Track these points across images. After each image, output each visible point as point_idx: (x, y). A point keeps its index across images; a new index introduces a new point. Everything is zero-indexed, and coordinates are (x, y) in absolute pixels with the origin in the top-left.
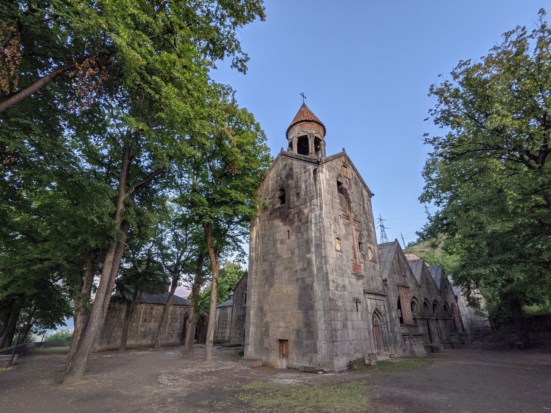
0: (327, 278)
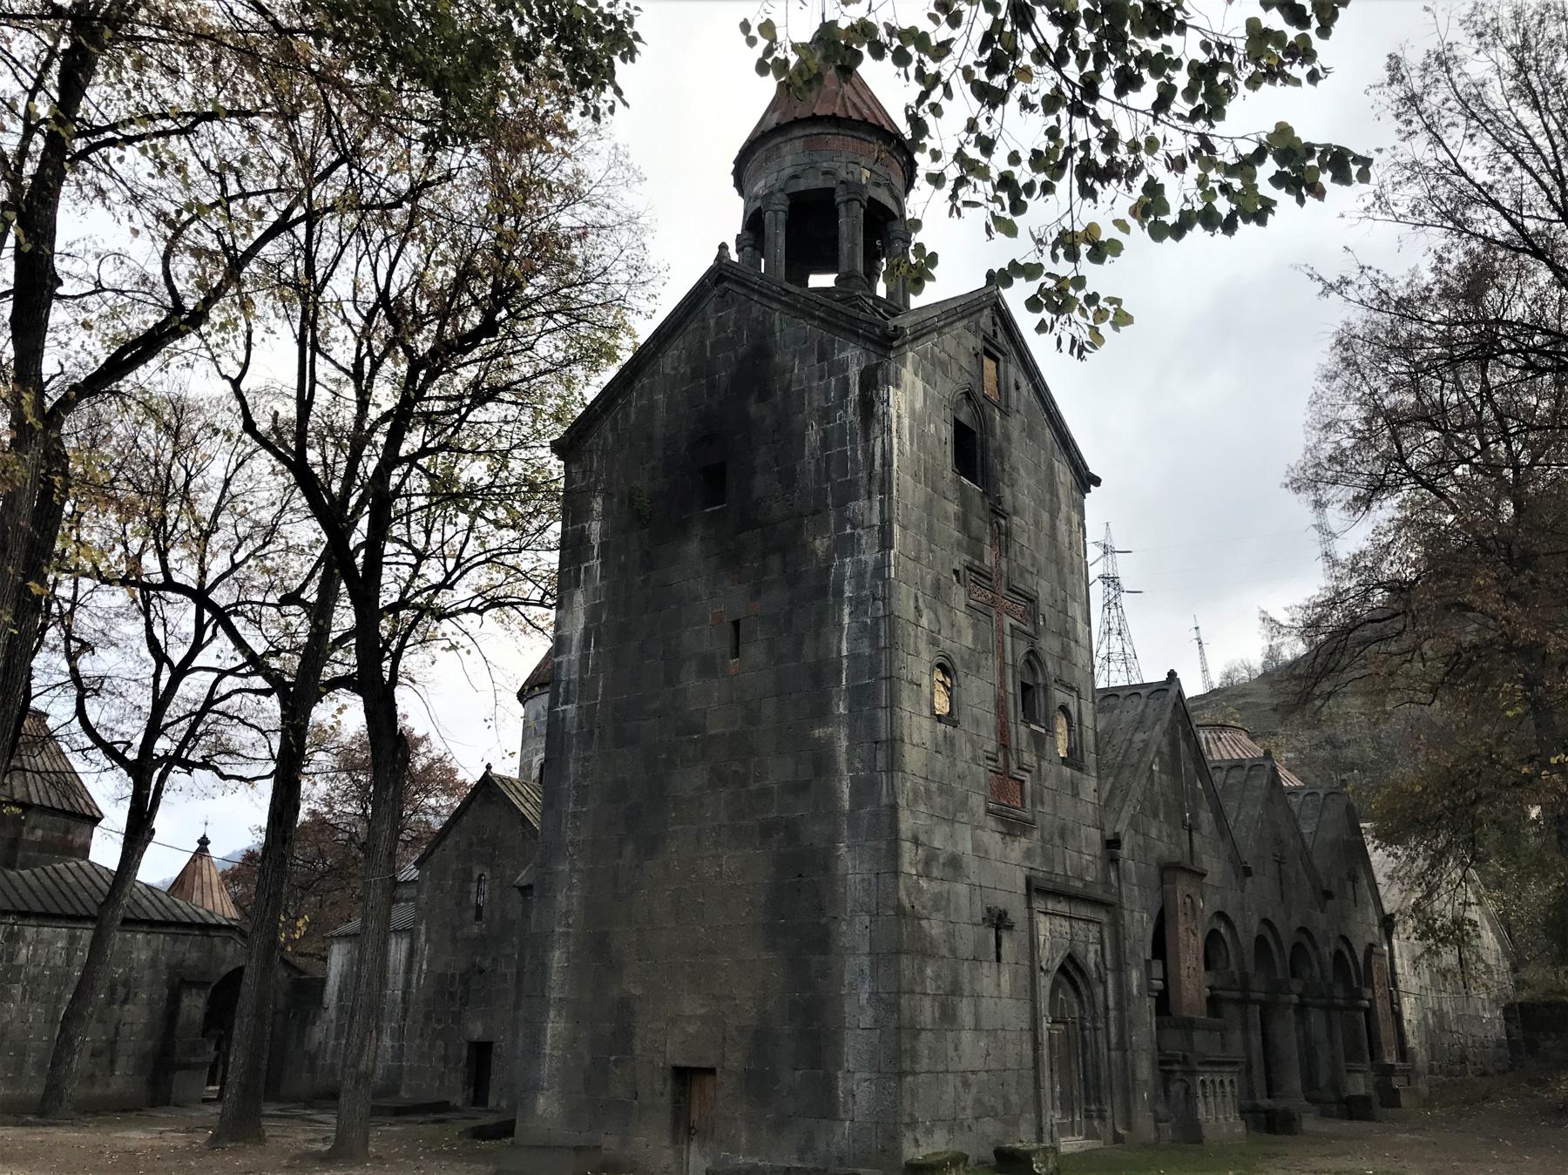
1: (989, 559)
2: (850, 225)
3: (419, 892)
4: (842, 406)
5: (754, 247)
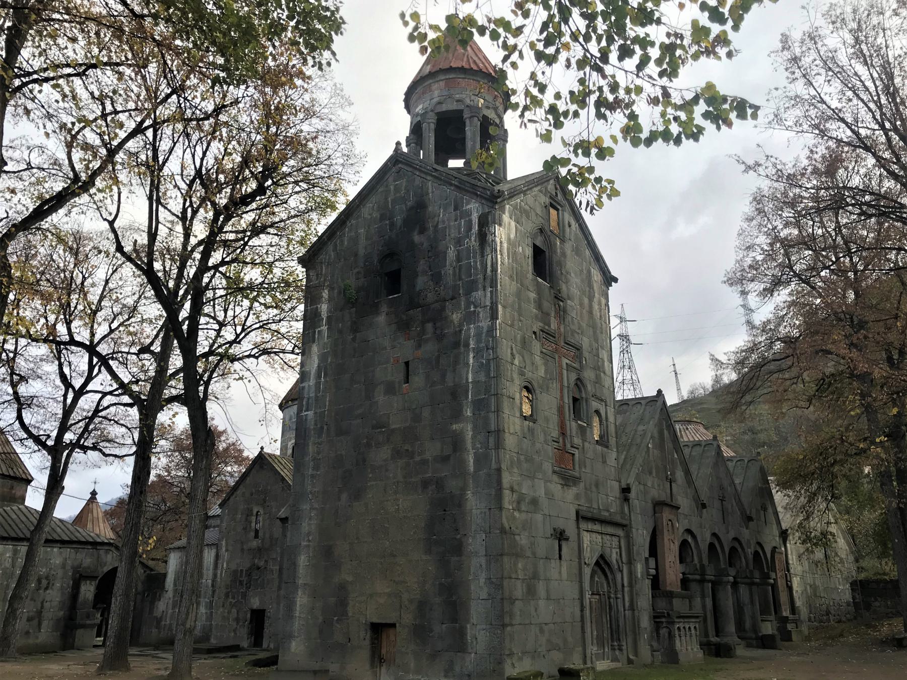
0: (499, 482)
1: (554, 325)
2: (472, 131)
3: (222, 522)
4: (468, 236)
5: (416, 143)
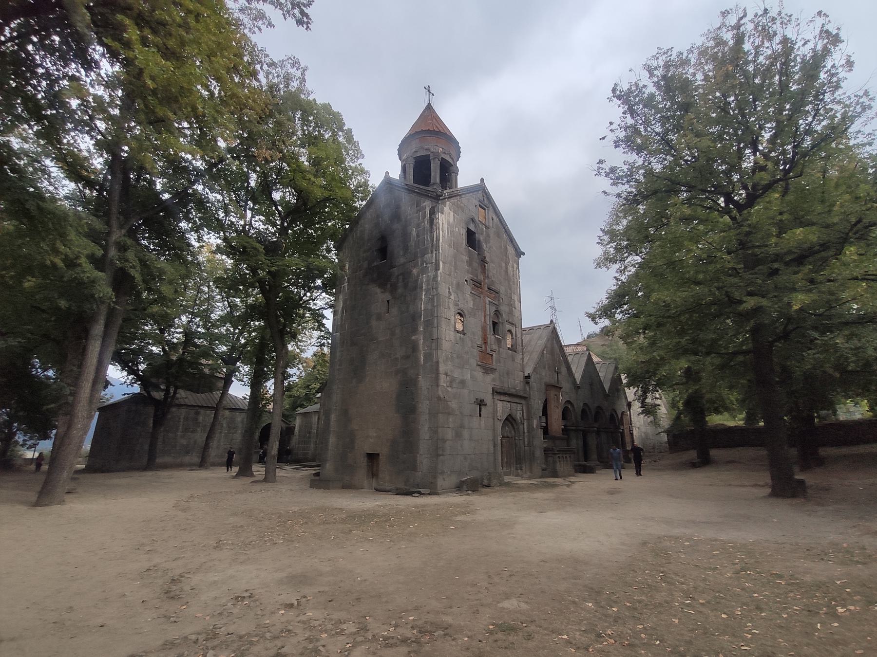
0: (437, 369)
